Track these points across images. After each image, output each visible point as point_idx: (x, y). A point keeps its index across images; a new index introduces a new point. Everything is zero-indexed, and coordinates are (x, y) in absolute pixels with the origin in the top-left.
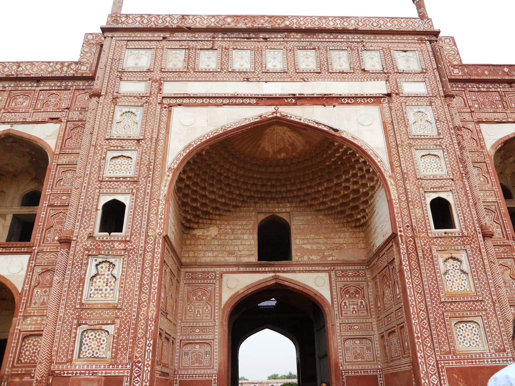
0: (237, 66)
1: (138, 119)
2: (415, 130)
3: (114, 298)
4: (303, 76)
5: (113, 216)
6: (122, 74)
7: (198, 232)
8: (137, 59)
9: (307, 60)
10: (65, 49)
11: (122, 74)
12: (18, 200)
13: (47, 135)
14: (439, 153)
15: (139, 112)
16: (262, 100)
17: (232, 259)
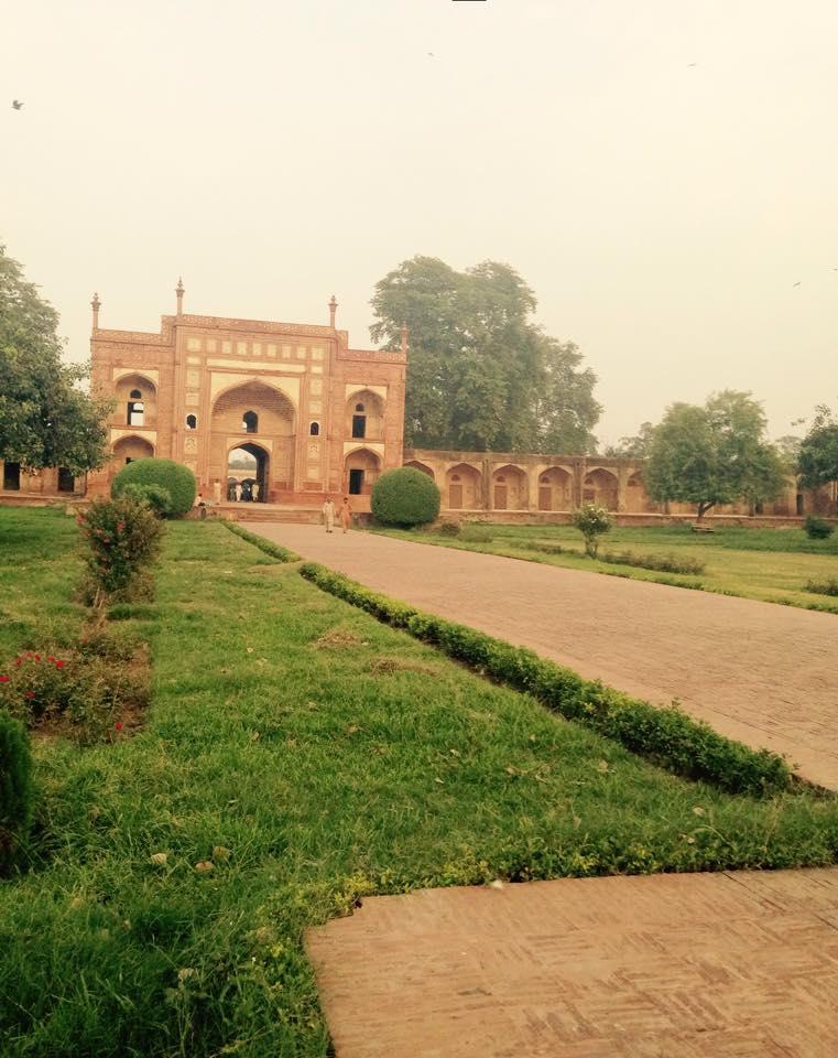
0: (239, 352)
1: (198, 377)
2: (313, 392)
3: (195, 452)
4: (269, 360)
5: (192, 421)
6: (189, 353)
7: (216, 417)
8: (194, 344)
9: (272, 351)
10: (154, 327)
11: (189, 353)
12: (129, 395)
13: (153, 375)
14: (320, 403)
15: (197, 373)
16: (251, 372)
17: (231, 431)
